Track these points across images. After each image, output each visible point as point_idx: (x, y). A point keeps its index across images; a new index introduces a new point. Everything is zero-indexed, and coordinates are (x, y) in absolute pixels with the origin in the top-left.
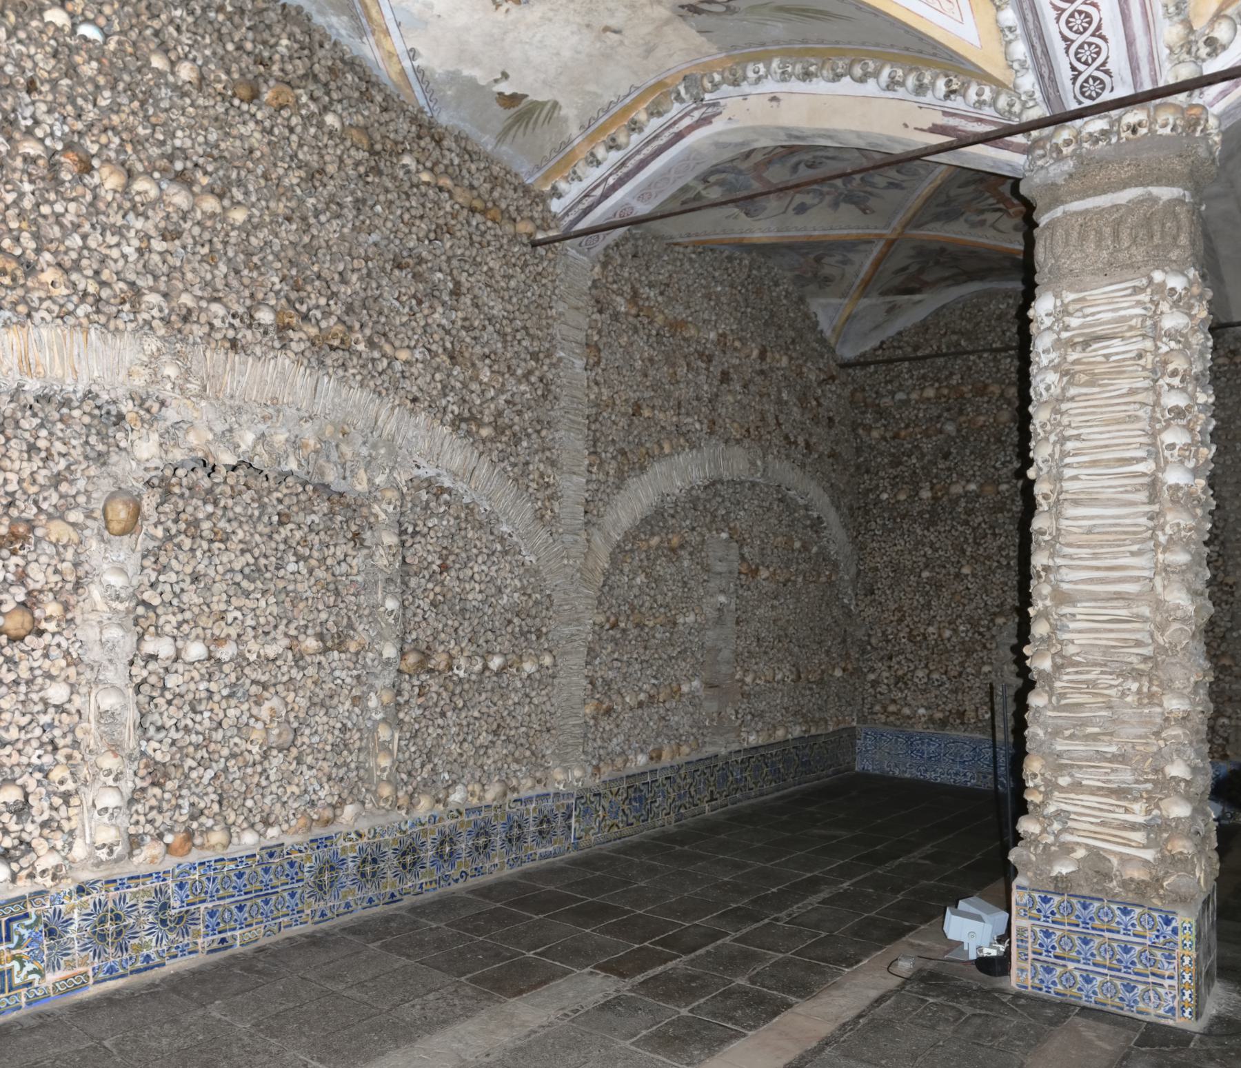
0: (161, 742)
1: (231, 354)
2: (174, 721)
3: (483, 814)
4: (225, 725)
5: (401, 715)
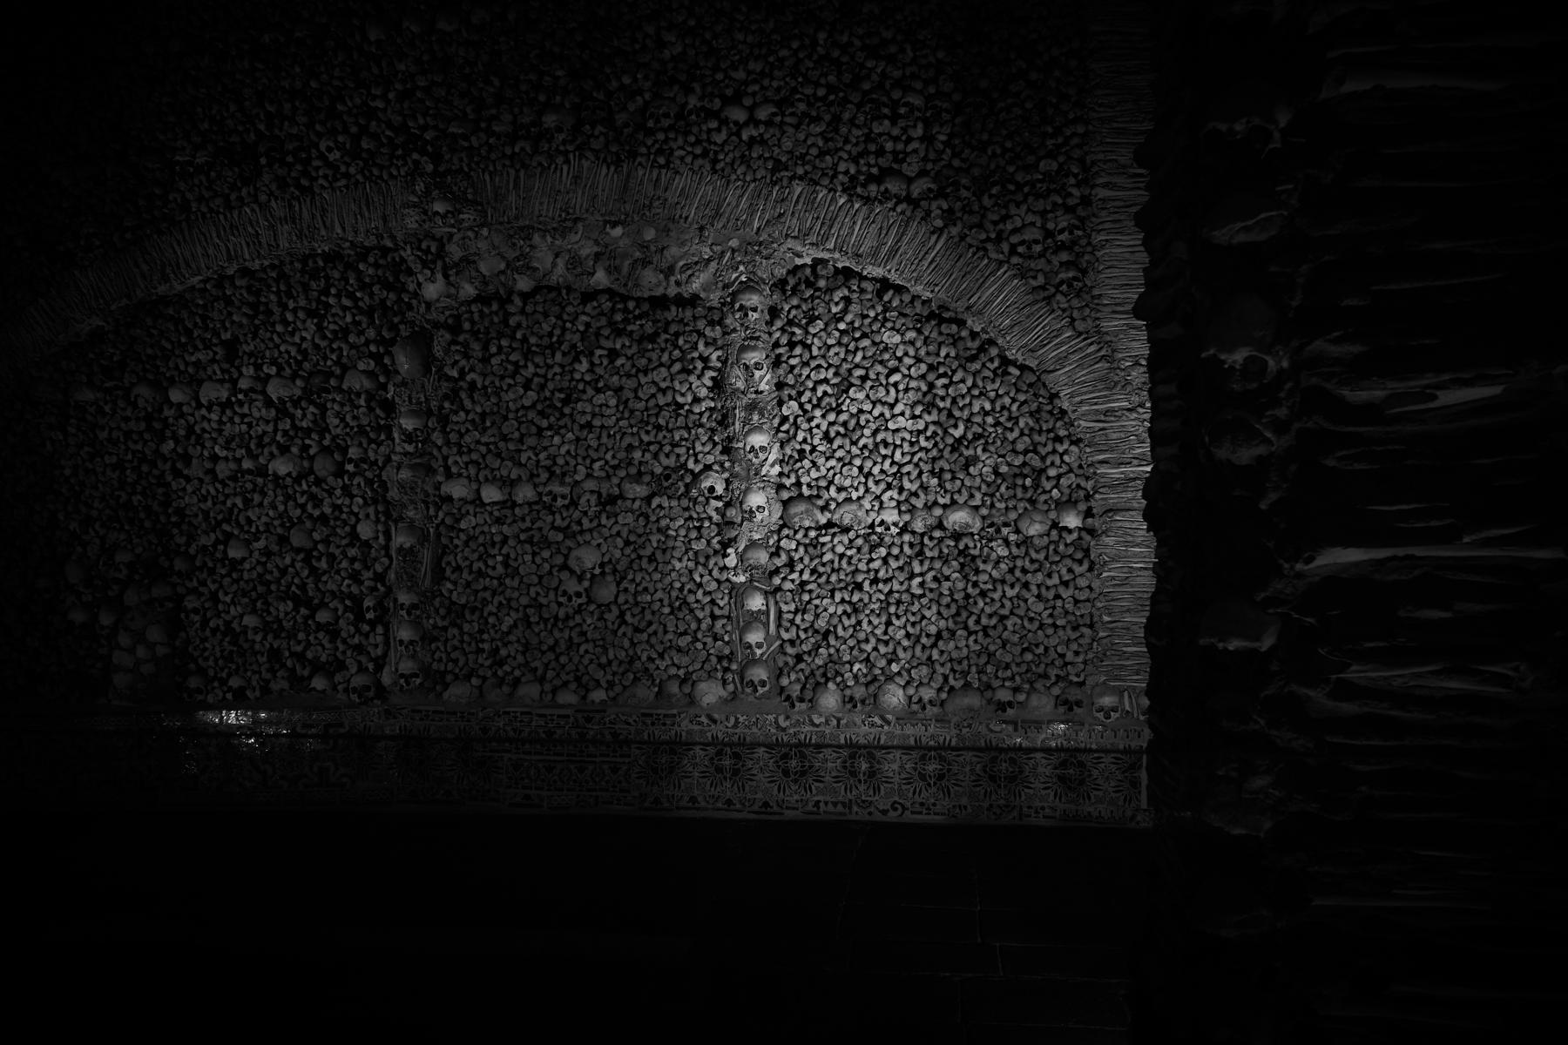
2: (467, 563)
3: (931, 730)
5: (777, 581)
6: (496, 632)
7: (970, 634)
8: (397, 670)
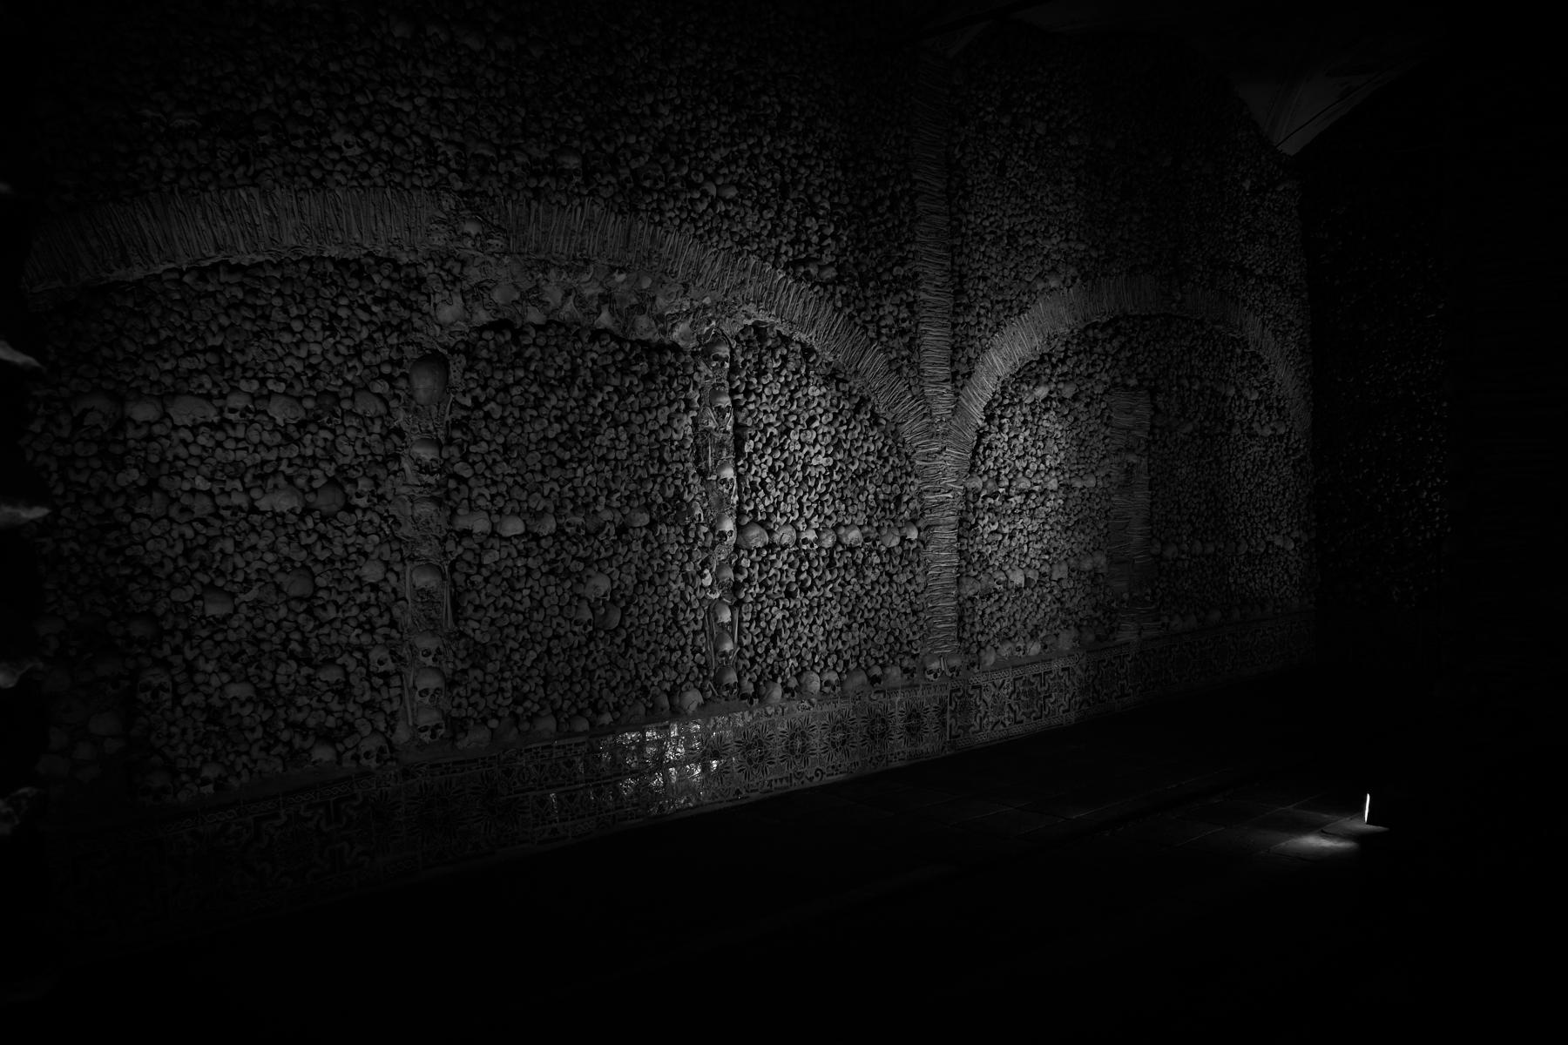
0: (479, 621)
1: (534, 204)
2: (491, 599)
4: (545, 603)
6: (519, 668)
7: (861, 625)
8: (415, 725)
